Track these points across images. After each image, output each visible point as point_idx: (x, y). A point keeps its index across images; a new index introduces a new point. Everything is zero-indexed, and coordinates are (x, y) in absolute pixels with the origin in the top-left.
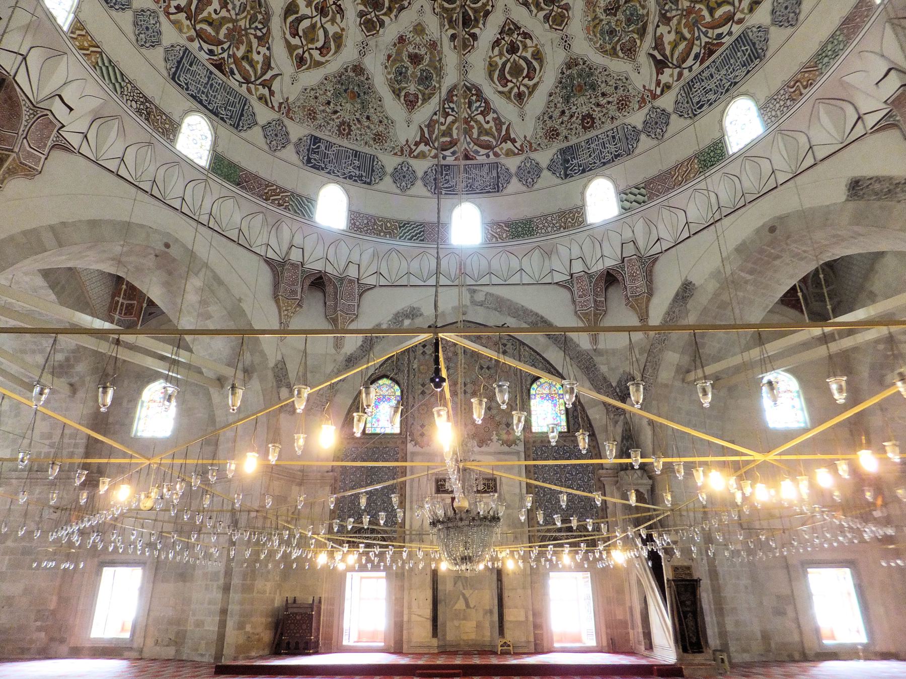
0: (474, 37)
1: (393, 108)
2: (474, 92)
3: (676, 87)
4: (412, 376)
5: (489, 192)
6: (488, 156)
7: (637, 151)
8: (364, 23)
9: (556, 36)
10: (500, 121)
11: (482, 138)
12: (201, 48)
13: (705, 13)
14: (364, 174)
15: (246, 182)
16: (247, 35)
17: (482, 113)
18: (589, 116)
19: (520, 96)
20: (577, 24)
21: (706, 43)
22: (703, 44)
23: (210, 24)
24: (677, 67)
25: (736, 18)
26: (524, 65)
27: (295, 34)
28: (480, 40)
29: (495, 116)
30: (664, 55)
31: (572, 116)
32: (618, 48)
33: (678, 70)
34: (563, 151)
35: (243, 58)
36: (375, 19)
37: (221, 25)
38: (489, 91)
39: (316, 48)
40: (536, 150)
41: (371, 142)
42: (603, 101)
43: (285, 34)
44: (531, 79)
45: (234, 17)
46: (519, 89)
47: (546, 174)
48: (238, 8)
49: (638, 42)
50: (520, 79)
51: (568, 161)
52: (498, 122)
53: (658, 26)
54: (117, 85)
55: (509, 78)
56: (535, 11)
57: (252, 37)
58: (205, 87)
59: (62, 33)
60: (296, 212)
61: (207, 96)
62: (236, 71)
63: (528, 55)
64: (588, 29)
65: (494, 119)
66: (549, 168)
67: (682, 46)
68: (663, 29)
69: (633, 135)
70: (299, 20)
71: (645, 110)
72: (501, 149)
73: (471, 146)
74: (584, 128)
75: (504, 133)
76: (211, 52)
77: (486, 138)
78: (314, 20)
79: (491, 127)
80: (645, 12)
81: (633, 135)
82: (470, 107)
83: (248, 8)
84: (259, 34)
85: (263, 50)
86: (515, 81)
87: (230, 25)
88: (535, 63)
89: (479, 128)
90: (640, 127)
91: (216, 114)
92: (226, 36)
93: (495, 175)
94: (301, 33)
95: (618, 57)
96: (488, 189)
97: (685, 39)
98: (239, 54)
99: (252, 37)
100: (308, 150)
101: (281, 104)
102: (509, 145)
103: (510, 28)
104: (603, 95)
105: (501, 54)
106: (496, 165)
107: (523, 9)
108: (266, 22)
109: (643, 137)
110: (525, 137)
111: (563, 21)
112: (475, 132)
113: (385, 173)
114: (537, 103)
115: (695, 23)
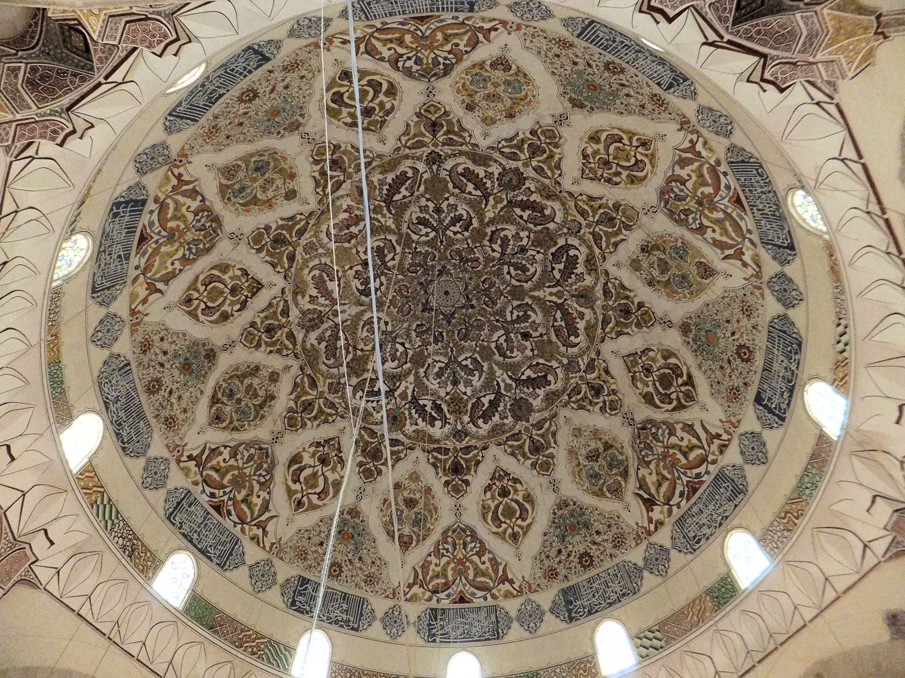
0: (467, 483)
1: (388, 550)
2: (468, 533)
3: (669, 522)
5: (489, 639)
6: (485, 599)
7: (643, 590)
8: (363, 472)
9: (544, 480)
10: (496, 561)
11: (478, 579)
12: (204, 491)
13: (679, 456)
14: (352, 619)
15: (220, 625)
16: (250, 481)
17: (477, 554)
18: (587, 554)
19: (514, 536)
20: (562, 470)
21: (688, 482)
22: (685, 483)
23: (217, 471)
24: (665, 504)
25: (709, 459)
26: (516, 507)
27: (296, 480)
28: (472, 485)
29: (491, 556)
30: (650, 494)
31: (569, 555)
32: (605, 489)
33: (667, 507)
34: (564, 592)
35: (243, 501)
36: (373, 468)
37: (227, 472)
38: (484, 531)
39: (315, 493)
40: (536, 591)
41: (363, 584)
42: (598, 539)
43: (286, 480)
44: (524, 520)
45: (241, 465)
46: (513, 529)
47: (548, 617)
48: (246, 458)
49: (623, 483)
50: (514, 520)
51: (571, 603)
52: (494, 562)
54: (109, 523)
55: (503, 520)
56: (522, 460)
57: (255, 482)
58: (199, 527)
59: (69, 474)
60: (270, 662)
61: (199, 535)
62: (233, 512)
63: (520, 498)
64: (573, 473)
65: (490, 560)
66: (552, 611)
67: (665, 485)
68: (643, 472)
69: (634, 574)
70: (301, 469)
71: (643, 546)
72: (499, 591)
73: (467, 588)
74: (583, 566)
75: (500, 573)
76: (212, 495)
77: (483, 579)
78: (316, 469)
79: (487, 568)
80: (624, 458)
81: (634, 574)
82: (465, 548)
83: (256, 458)
84: (262, 480)
85: (263, 494)
86: (508, 521)
87: (236, 472)
88: (527, 505)
89: (475, 569)
90: (641, 563)
91: (203, 552)
92: (230, 481)
93: (494, 619)
94: (302, 480)
95: (606, 497)
96: (487, 636)
97: (667, 479)
98: (240, 497)
99: (255, 482)
100: (294, 592)
101: (273, 544)
102: (507, 586)
103: (499, 474)
104: (598, 533)
105: (493, 498)
106: (494, 609)
107: (512, 459)
108: (270, 471)
109: (646, 574)
110: (523, 578)
111: (549, 468)
112: (471, 574)
113: (374, 618)
114: (532, 543)
115: (673, 465)
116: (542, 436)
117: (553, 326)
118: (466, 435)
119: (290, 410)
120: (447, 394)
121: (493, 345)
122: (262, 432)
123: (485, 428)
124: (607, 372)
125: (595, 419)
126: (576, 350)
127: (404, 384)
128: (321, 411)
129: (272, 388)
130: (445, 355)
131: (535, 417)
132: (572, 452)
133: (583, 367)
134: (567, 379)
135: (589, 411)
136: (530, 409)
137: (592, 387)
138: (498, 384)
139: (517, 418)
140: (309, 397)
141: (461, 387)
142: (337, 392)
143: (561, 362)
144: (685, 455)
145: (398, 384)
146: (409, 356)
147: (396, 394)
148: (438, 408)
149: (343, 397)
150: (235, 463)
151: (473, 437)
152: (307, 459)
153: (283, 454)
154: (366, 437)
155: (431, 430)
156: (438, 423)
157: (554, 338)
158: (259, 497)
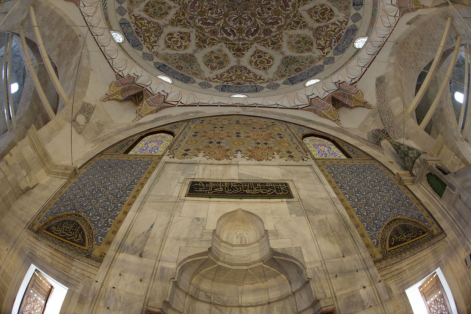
4: (186, 130)
9: (278, 52)
13: (332, 32)
27: (170, 39)
43: (166, 38)
53: (317, 41)
67: (328, 42)
78: (178, 40)
84: (156, 34)
116: (277, 39)
117: (280, 5)
118: (244, 40)
119: (173, 19)
120: (237, 27)
121: (256, 12)
122: (161, 22)
123: (251, 38)
124: (301, 16)
125: (299, 31)
126: (289, 12)
127: (219, 22)
128: (184, 23)
129: (168, 11)
130: (237, 15)
131: (273, 34)
132: (289, 43)
133: (292, 17)
134: (286, 21)
135: (295, 29)
136: (271, 32)
137: (295, 22)
138: (258, 24)
139: (265, 35)
140: (180, 18)
141: (243, 25)
142: (192, 19)
143: (283, 16)
144: (334, 31)
145: (217, 22)
146: (223, 13)
147: (216, 25)
148: (233, 31)
149: (194, 22)
150: (148, 26)
151: (247, 41)
152: (175, 35)
153: (166, 31)
154: (201, 35)
155: (228, 37)
156: (232, 36)
157: (280, 9)
158: (154, 38)
